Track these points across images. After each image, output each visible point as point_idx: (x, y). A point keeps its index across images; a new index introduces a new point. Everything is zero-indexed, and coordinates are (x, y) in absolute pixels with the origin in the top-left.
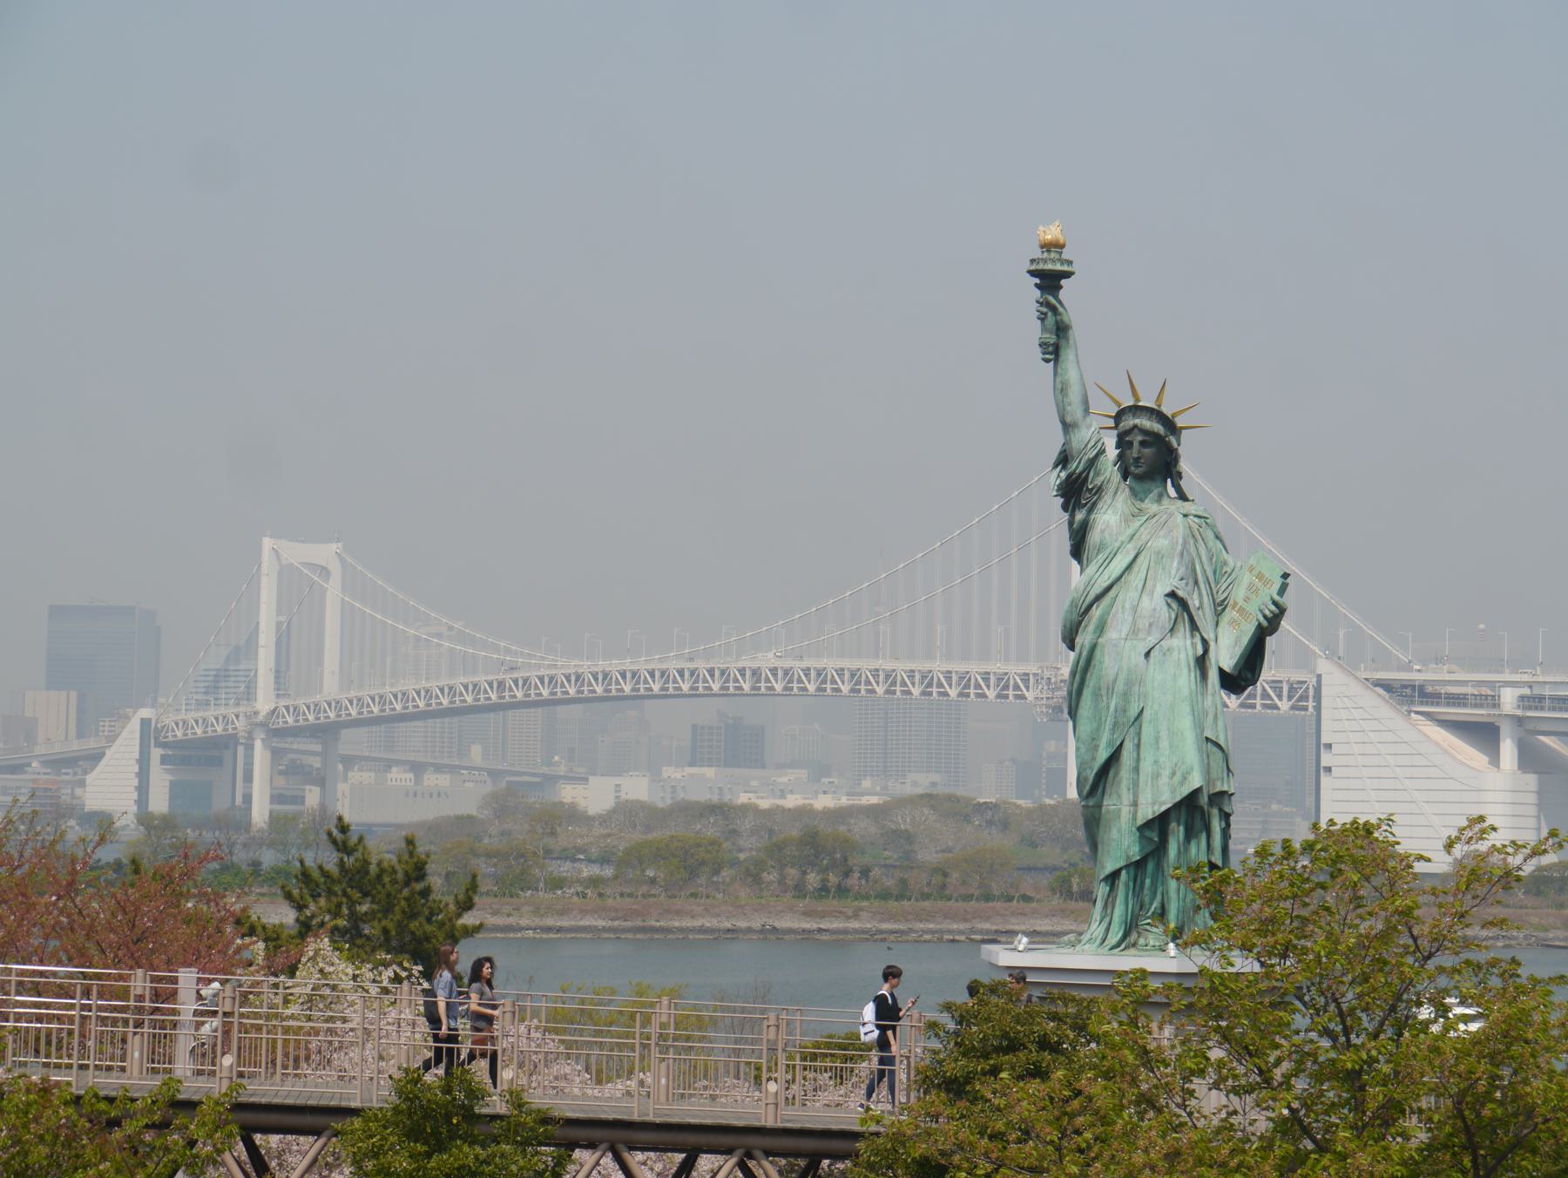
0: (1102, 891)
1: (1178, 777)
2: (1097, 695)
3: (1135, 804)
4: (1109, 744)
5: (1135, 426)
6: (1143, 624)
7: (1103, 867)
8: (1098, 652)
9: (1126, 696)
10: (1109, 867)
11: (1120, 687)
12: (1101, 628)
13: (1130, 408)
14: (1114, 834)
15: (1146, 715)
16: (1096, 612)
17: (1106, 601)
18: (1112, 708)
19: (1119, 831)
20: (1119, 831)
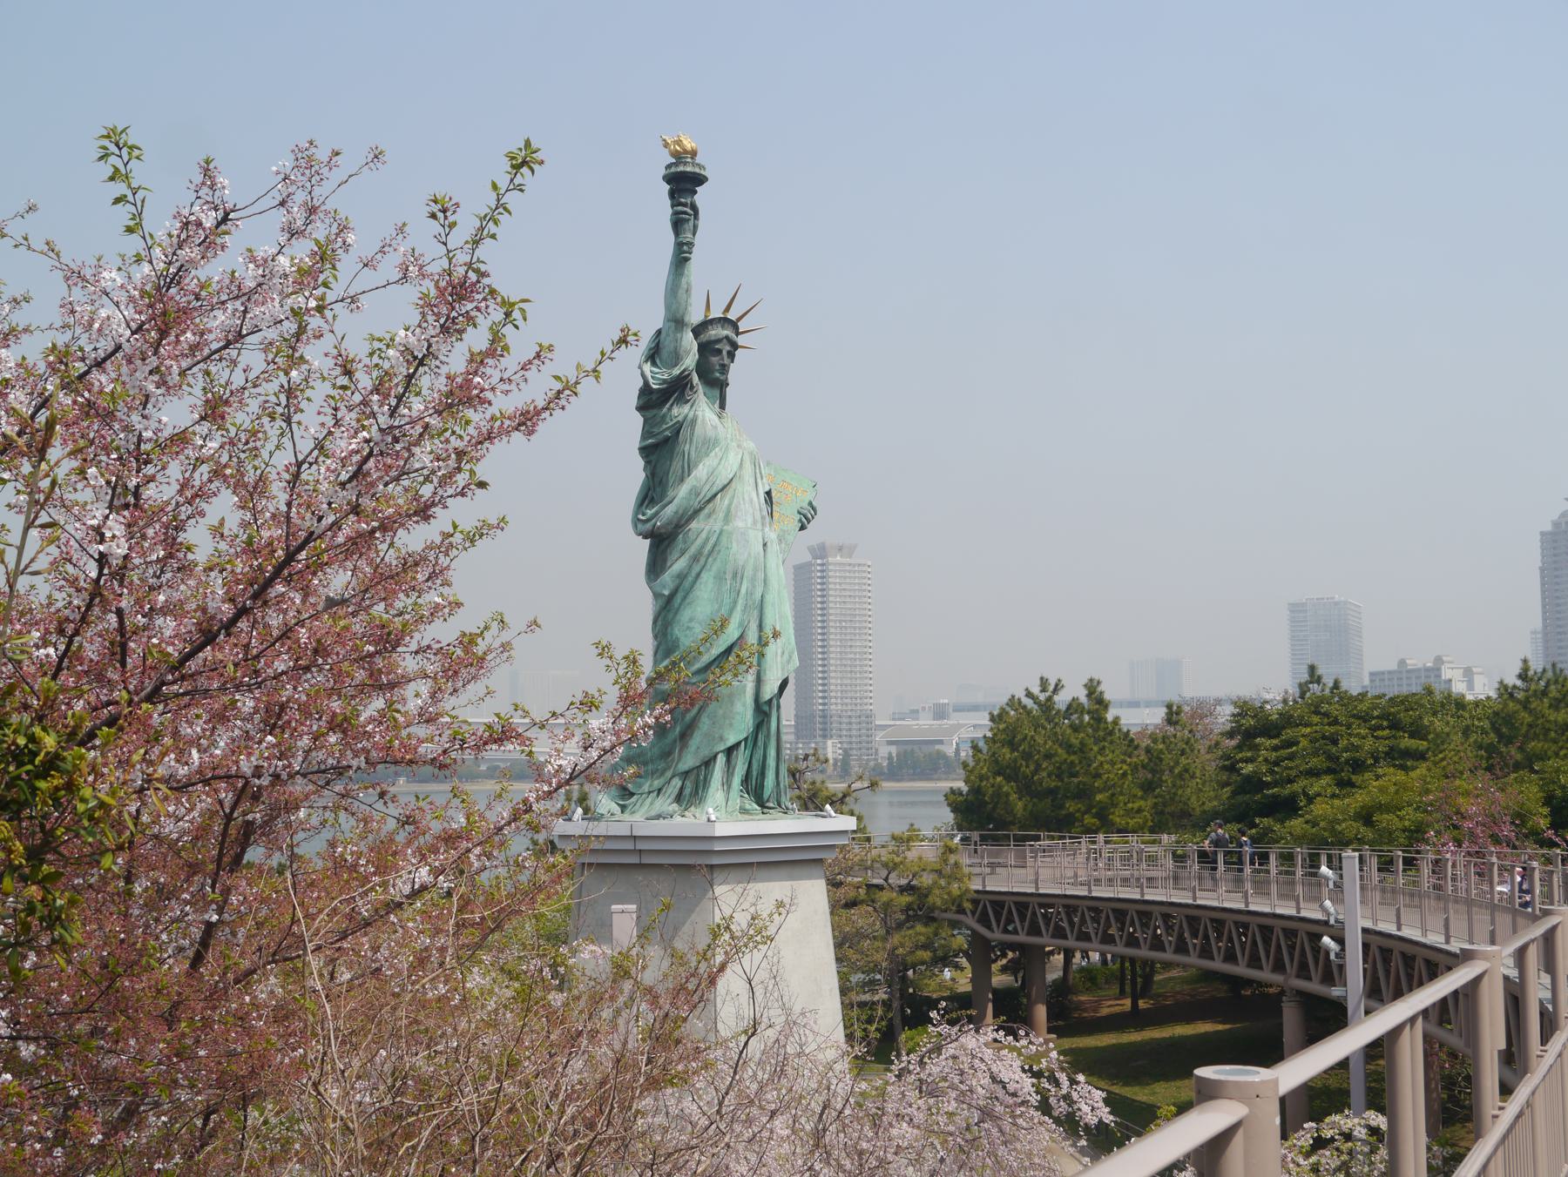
0: (721, 759)
1: (786, 656)
2: (720, 578)
3: (759, 681)
4: (741, 624)
5: (727, 337)
6: (758, 517)
7: (721, 739)
8: (724, 539)
9: (753, 580)
10: (731, 741)
11: (749, 572)
12: (727, 518)
13: (720, 319)
14: (738, 707)
15: (769, 598)
16: (721, 503)
17: (730, 491)
18: (743, 591)
19: (744, 705)
20: (744, 705)
